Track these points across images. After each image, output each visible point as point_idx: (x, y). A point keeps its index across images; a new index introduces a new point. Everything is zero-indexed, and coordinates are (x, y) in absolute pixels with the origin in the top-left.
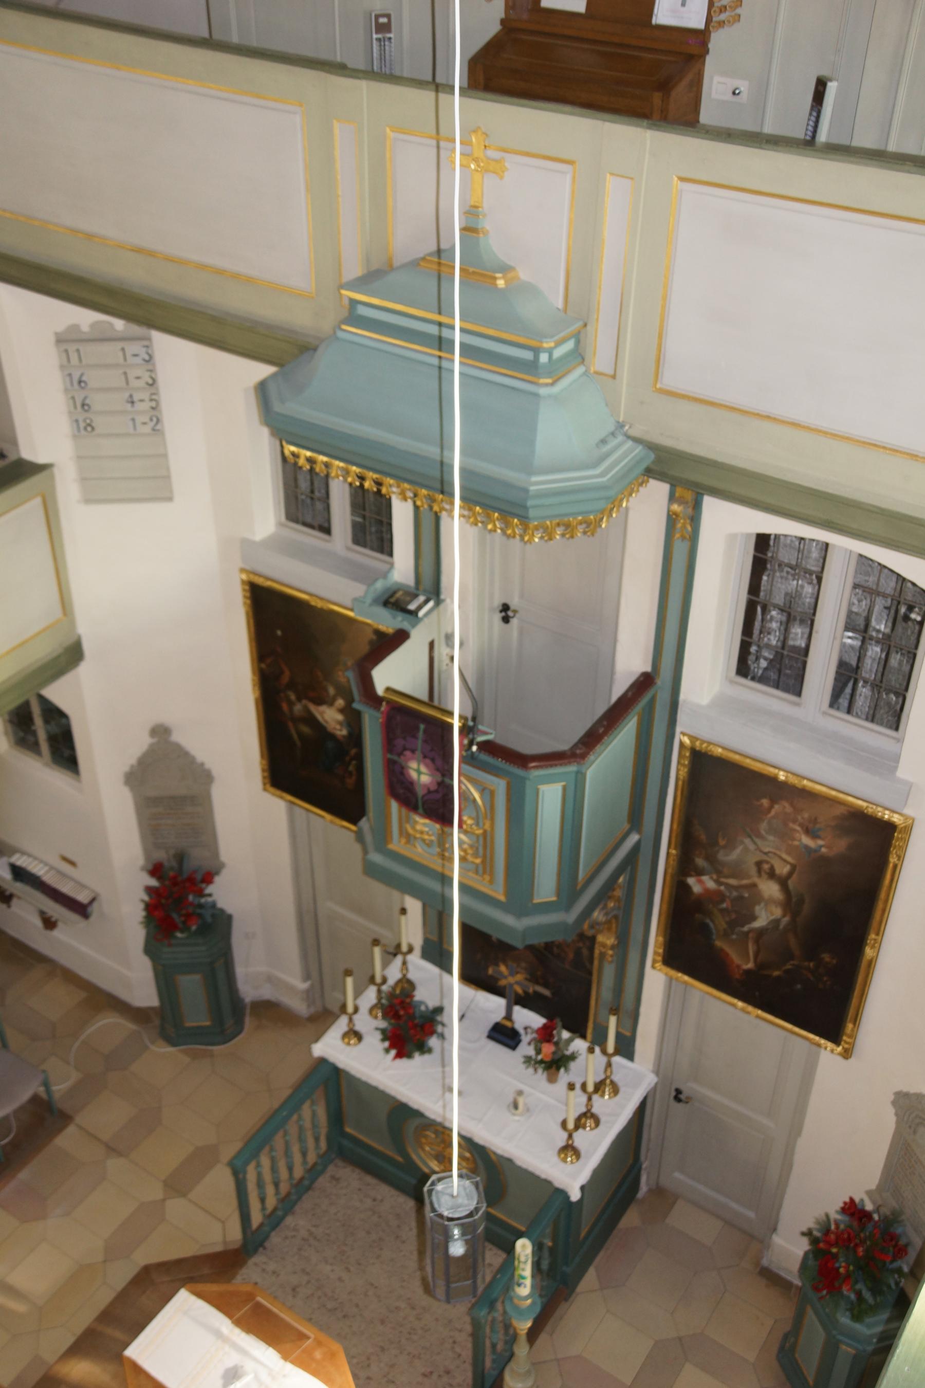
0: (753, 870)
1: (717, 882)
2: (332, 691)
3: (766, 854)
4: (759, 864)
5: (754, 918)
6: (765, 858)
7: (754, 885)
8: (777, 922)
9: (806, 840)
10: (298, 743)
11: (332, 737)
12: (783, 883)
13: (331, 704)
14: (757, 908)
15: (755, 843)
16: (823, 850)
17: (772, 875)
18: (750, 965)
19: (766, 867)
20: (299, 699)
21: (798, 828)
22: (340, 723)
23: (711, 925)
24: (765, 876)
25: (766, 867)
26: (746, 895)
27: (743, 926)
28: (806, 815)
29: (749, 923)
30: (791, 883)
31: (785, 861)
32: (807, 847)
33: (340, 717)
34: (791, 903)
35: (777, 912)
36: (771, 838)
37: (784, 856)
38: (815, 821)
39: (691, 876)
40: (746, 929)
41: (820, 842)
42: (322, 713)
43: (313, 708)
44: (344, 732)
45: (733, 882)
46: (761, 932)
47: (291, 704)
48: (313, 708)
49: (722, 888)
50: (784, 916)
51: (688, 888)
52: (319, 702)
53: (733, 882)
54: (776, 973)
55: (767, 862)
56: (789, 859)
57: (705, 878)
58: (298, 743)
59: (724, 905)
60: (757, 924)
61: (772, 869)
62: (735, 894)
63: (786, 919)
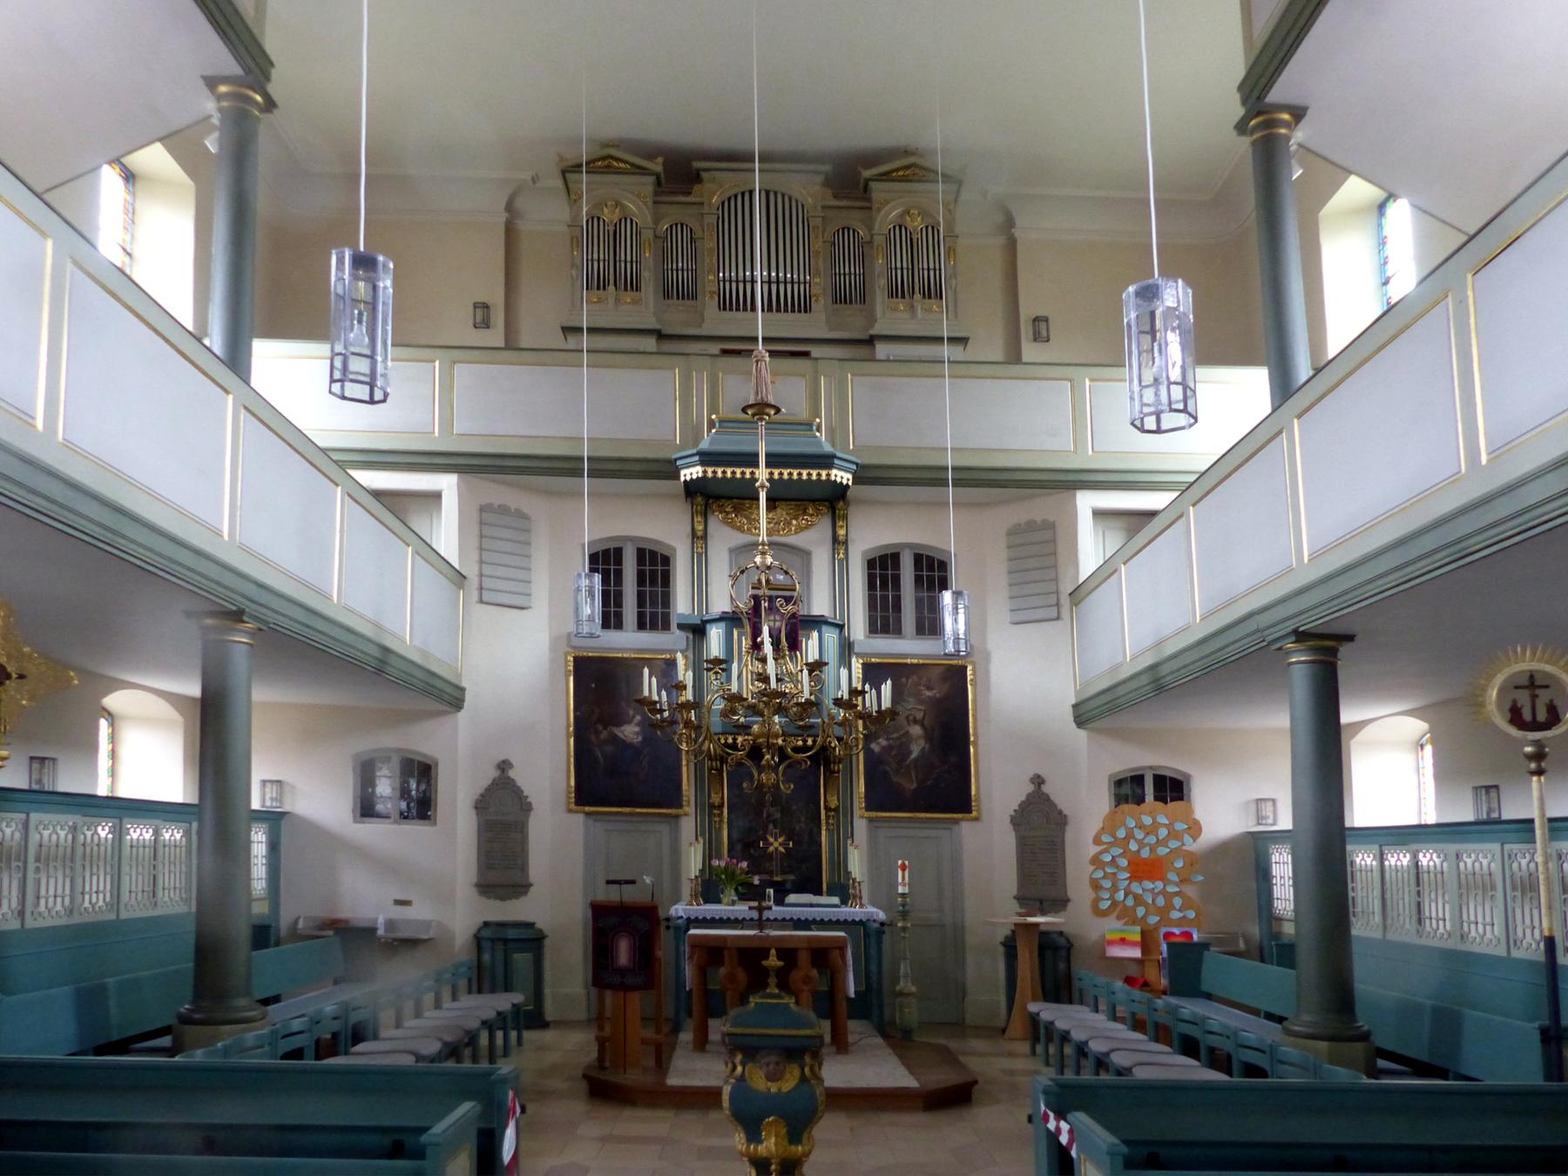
0: (905, 723)
1: (888, 739)
2: (631, 712)
3: (909, 710)
4: (907, 718)
5: (910, 753)
6: (909, 712)
7: (908, 732)
8: (924, 748)
9: (928, 693)
10: (601, 760)
11: (630, 746)
12: (921, 723)
13: (629, 722)
14: (911, 746)
15: (903, 706)
16: (938, 695)
17: (915, 721)
18: (915, 785)
19: (911, 718)
20: (605, 728)
21: (922, 688)
22: (637, 733)
23: (888, 769)
24: (912, 724)
25: (911, 718)
26: (904, 740)
27: (906, 760)
28: (925, 679)
29: (908, 757)
30: (925, 722)
31: (921, 710)
32: (929, 697)
33: (637, 729)
34: (928, 736)
35: (922, 743)
36: (910, 699)
37: (920, 707)
38: (930, 680)
39: (871, 742)
40: (908, 762)
41: (935, 691)
42: (623, 732)
43: (616, 731)
44: (640, 739)
45: (895, 735)
46: (916, 760)
47: (597, 733)
48: (616, 731)
49: (891, 741)
50: (926, 743)
51: (872, 751)
52: (619, 724)
53: (895, 735)
54: (929, 783)
55: (911, 715)
56: (923, 708)
57: (880, 740)
58: (601, 760)
59: (894, 753)
60: (914, 755)
61: (915, 718)
62: (898, 742)
63: (927, 747)
